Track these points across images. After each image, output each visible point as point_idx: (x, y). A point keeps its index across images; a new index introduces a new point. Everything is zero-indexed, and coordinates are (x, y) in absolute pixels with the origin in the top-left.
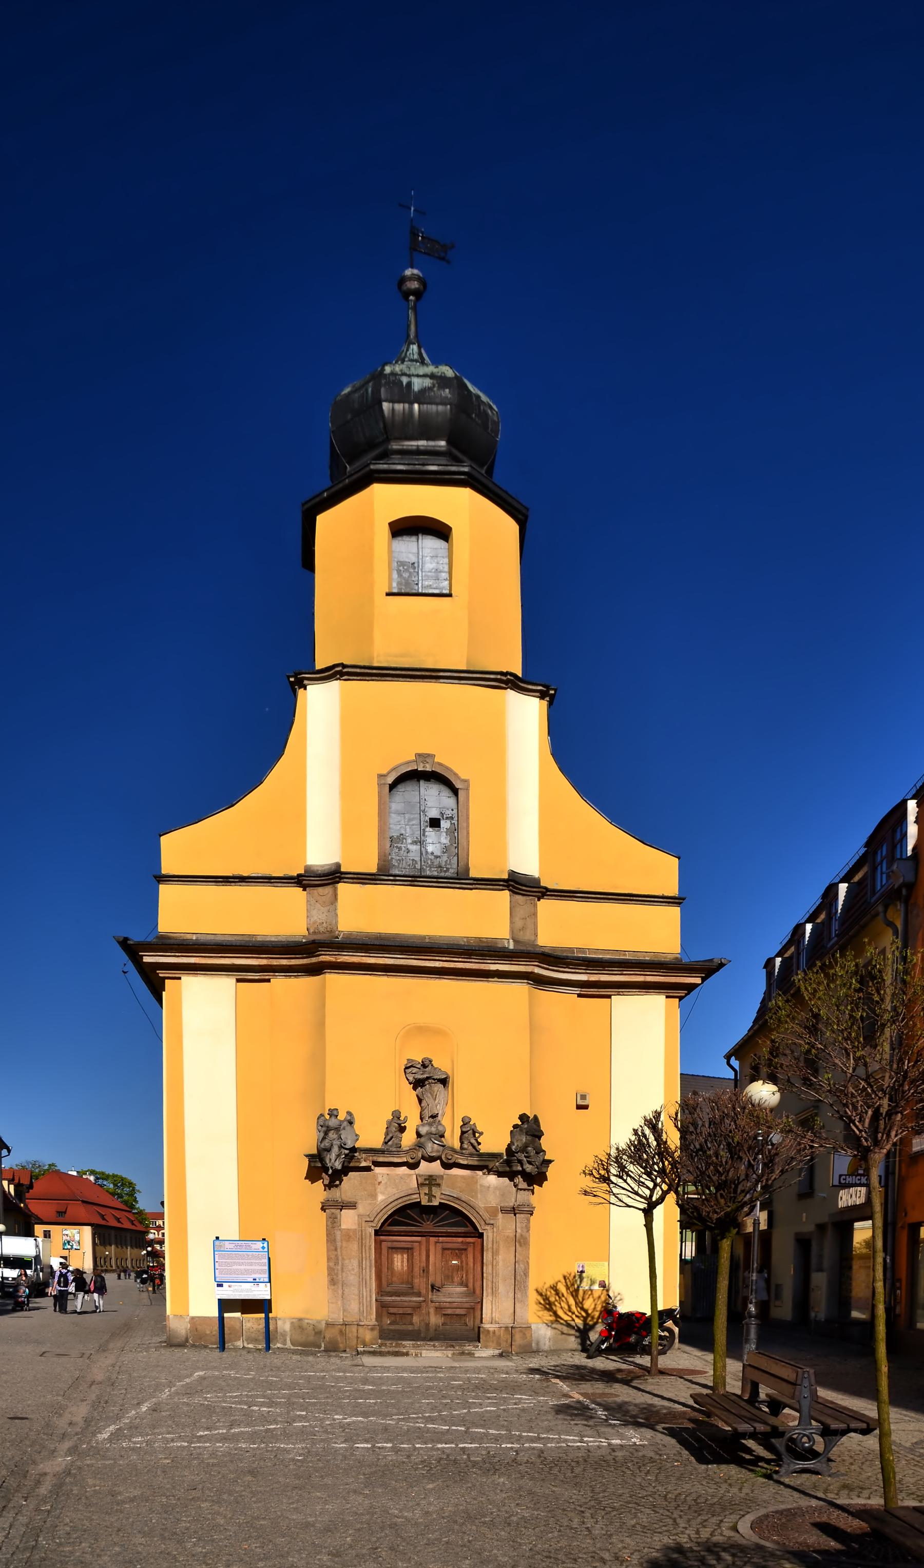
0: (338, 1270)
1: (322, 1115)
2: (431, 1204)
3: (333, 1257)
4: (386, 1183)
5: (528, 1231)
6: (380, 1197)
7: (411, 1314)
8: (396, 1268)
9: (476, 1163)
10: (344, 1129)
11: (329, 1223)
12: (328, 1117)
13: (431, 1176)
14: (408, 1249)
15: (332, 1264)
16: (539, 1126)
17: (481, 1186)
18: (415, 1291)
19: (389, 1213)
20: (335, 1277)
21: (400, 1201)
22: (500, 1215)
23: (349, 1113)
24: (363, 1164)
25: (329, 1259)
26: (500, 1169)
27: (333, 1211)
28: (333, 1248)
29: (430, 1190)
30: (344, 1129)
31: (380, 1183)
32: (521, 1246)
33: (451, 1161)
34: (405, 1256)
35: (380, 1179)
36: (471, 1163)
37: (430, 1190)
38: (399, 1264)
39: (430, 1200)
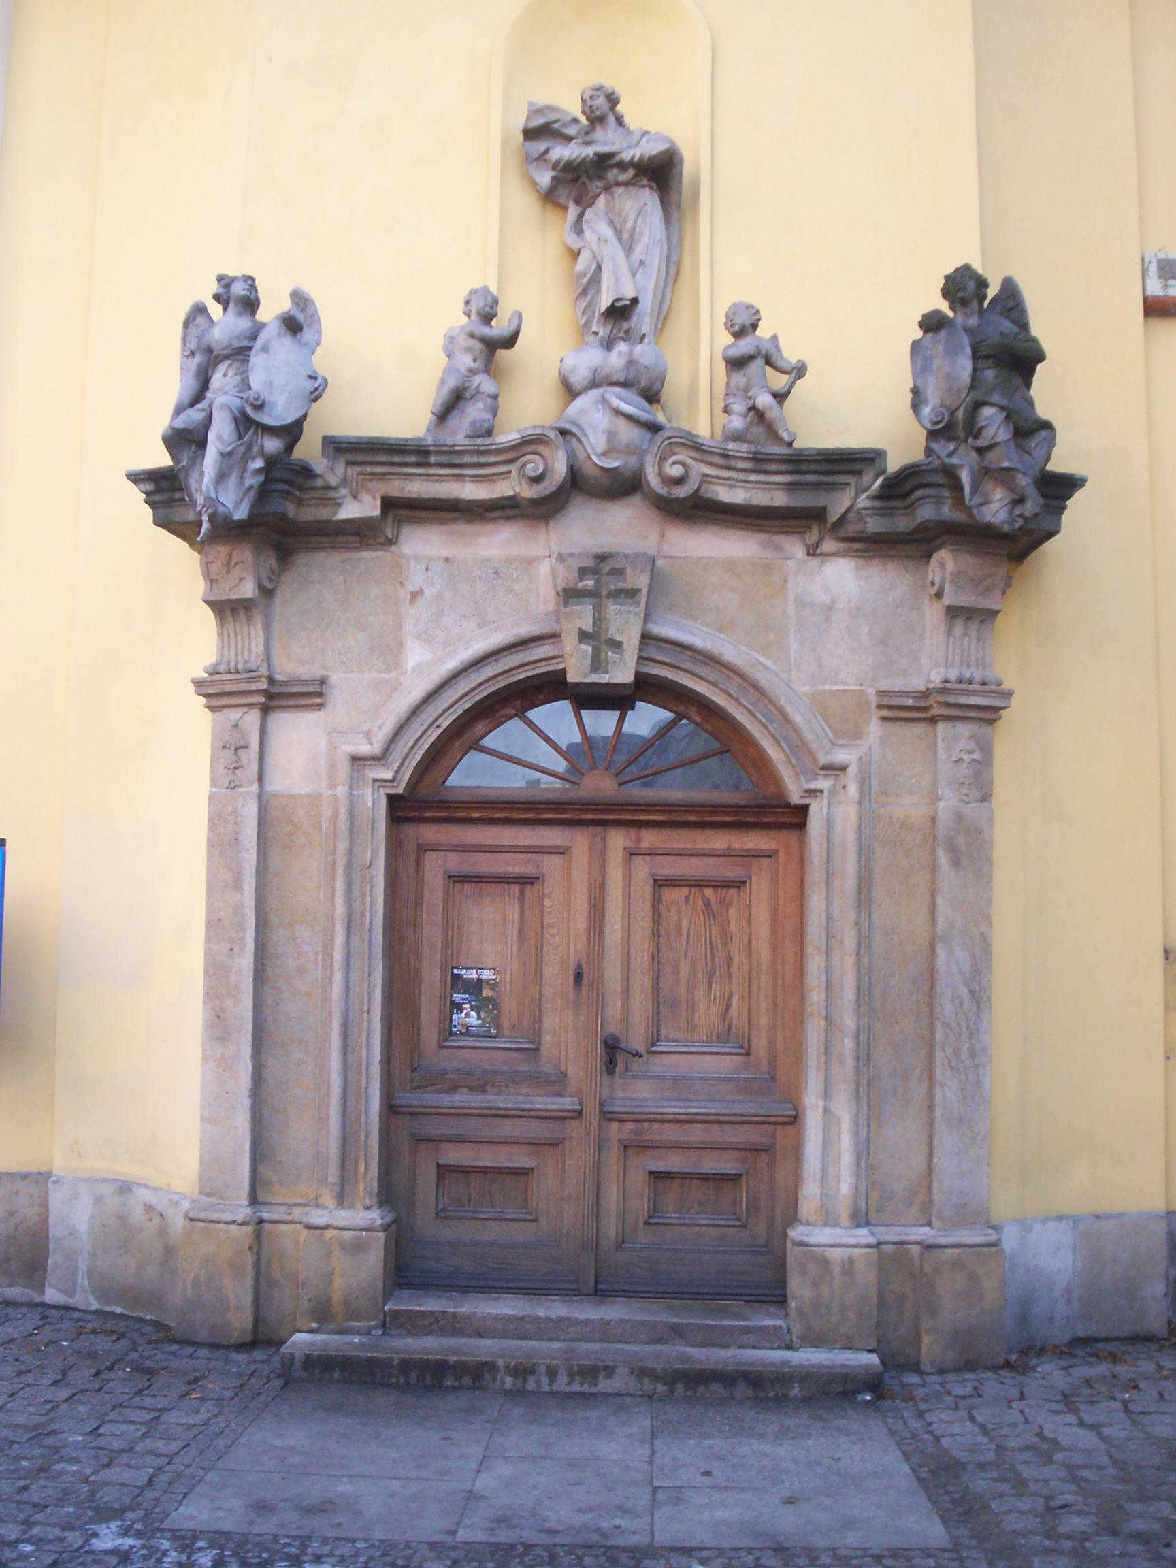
1: (199, 310)
2: (604, 678)
4: (439, 596)
5: (985, 798)
9: (779, 499)
11: (221, 771)
12: (215, 310)
13: (602, 558)
16: (1024, 326)
17: (800, 603)
19: (446, 723)
20: (229, 1002)
21: (489, 671)
22: (874, 729)
23: (299, 298)
24: (350, 511)
25: (213, 925)
26: (874, 525)
27: (235, 715)
29: (599, 618)
30: (265, 349)
31: (415, 596)
32: (956, 864)
33: (681, 492)
35: (416, 579)
36: (762, 498)
37: (599, 618)
39: (597, 664)
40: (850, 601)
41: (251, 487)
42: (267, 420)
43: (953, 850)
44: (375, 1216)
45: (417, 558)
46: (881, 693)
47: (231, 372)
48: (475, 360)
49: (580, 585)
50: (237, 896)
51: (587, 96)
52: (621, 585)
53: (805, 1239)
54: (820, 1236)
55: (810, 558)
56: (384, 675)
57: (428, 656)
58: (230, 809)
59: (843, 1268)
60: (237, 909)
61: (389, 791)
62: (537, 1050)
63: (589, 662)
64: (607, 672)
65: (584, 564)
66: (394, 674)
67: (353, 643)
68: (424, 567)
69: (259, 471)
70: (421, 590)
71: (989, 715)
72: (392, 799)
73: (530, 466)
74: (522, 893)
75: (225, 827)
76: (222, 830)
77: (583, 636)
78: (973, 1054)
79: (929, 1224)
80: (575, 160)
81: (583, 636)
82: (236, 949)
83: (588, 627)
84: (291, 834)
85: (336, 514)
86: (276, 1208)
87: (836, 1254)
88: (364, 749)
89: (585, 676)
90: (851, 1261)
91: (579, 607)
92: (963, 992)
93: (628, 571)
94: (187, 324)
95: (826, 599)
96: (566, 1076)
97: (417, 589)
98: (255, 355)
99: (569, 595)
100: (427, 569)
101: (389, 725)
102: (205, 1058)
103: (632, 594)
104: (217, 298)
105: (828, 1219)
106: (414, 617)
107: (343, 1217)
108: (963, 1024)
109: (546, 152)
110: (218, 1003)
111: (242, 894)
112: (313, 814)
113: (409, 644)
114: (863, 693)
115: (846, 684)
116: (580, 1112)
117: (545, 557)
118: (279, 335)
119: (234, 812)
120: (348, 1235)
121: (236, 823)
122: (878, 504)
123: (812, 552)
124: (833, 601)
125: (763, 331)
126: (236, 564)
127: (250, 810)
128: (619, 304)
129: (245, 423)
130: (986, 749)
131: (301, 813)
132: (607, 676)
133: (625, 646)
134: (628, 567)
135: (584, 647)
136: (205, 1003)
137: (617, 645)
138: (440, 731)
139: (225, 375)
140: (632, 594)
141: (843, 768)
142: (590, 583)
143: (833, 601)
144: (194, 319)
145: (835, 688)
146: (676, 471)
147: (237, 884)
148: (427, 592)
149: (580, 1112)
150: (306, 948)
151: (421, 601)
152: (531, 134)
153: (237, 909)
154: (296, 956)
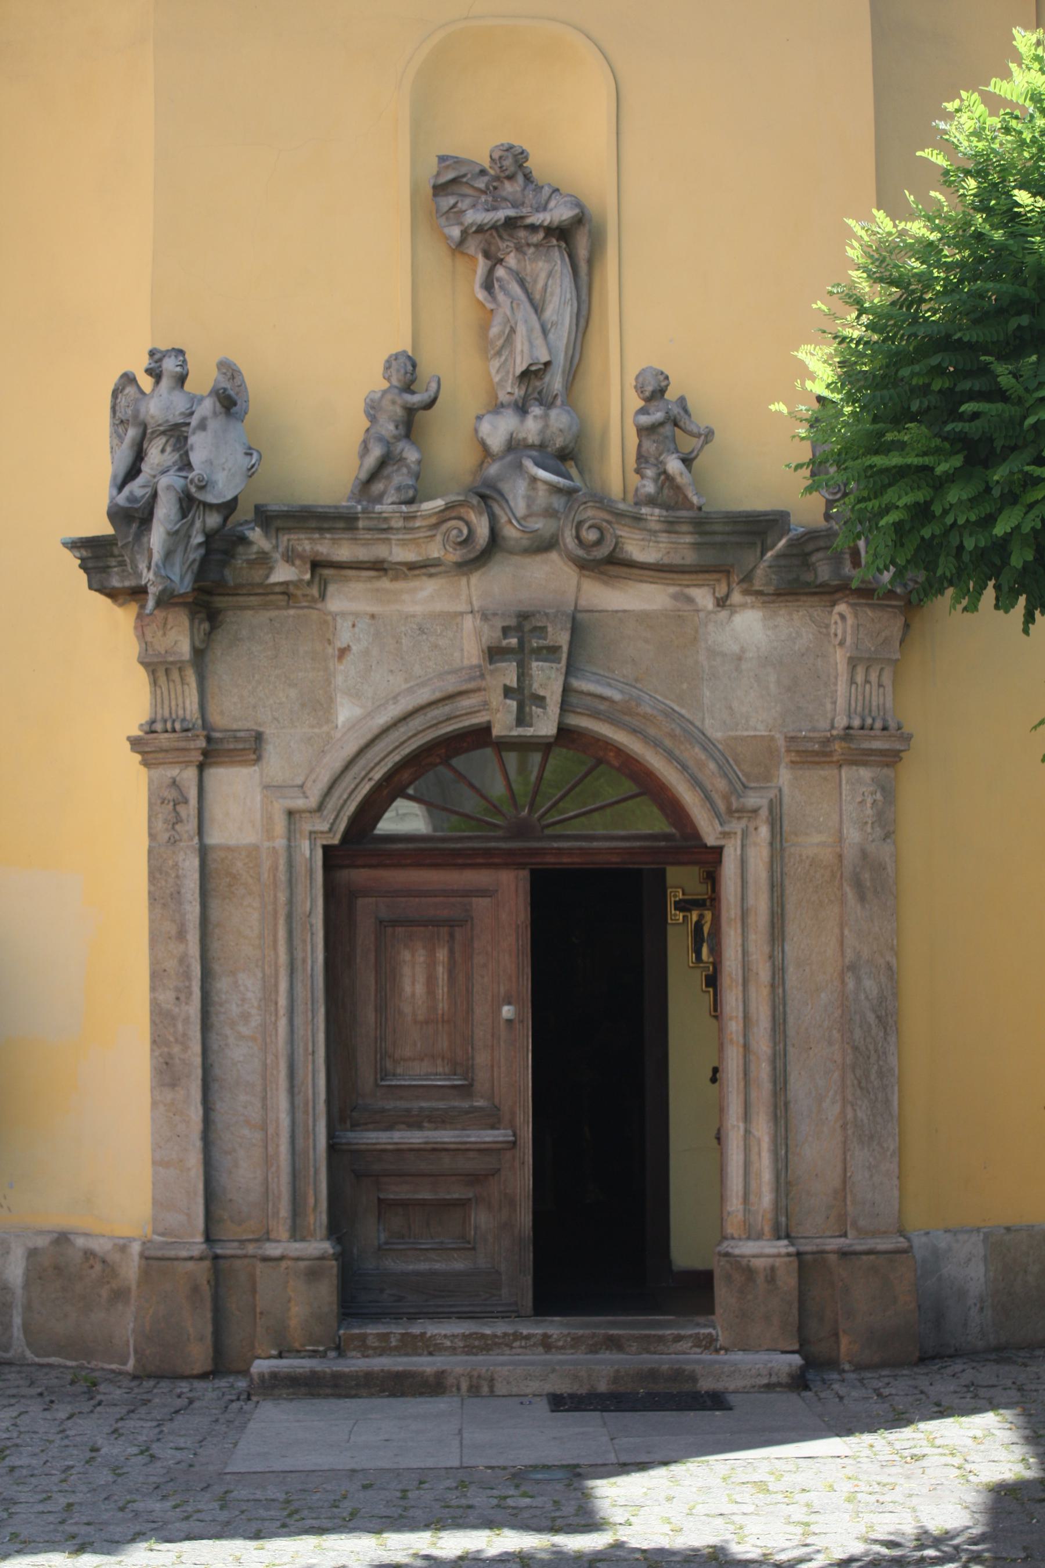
0: (187, 1020)
1: (128, 379)
2: (529, 731)
3: (171, 964)
4: (366, 652)
6: (345, 712)
7: (462, 1204)
8: (407, 1009)
10: (202, 426)
11: (160, 825)
12: (146, 383)
13: (524, 616)
14: (451, 924)
15: (167, 997)
17: (712, 653)
18: (480, 1103)
19: (378, 775)
20: (176, 1049)
21: (416, 723)
23: (229, 369)
24: (282, 573)
25: (157, 976)
28: (173, 930)
29: (523, 674)
31: (343, 652)
32: (862, 898)
34: (442, 955)
35: (344, 636)
37: (523, 674)
38: (420, 989)
39: (521, 720)
40: (758, 648)
41: (194, 560)
42: (211, 498)
43: (858, 885)
44: (326, 1247)
45: (343, 614)
46: (791, 739)
47: (169, 449)
48: (397, 427)
49: (505, 643)
50: (182, 947)
51: (496, 156)
52: (542, 643)
53: (730, 1250)
54: (747, 1248)
55: (719, 609)
56: (316, 730)
57: (358, 711)
58: (171, 863)
59: (766, 1277)
60: (183, 960)
61: (325, 843)
62: (471, 1085)
63: (514, 716)
64: (531, 726)
65: (506, 624)
66: (325, 728)
67: (284, 699)
68: (350, 624)
69: (200, 545)
70: (349, 646)
71: (891, 758)
72: (328, 851)
73: (455, 532)
74: (452, 936)
75: (166, 881)
76: (163, 883)
77: (508, 692)
78: (881, 1074)
79: (845, 1235)
80: (486, 224)
81: (508, 692)
82: (183, 997)
83: (512, 681)
84: (230, 885)
85: (267, 576)
86: (228, 1245)
87: (759, 1263)
88: (300, 803)
89: (511, 729)
90: (773, 1269)
91: (504, 664)
92: (871, 1017)
93: (550, 629)
94: (115, 393)
95: (736, 648)
96: (499, 1110)
97: (344, 645)
98: (194, 433)
99: (494, 654)
100: (354, 626)
101: (325, 778)
102: (154, 1104)
103: (553, 651)
104: (149, 371)
105: (752, 1234)
106: (345, 673)
107: (296, 1248)
108: (871, 1047)
109: (455, 206)
110: (166, 1050)
111: (187, 945)
112: (251, 865)
113: (338, 699)
114: (772, 739)
115: (755, 729)
116: (514, 1143)
117: (467, 613)
118: (215, 414)
119: (176, 865)
120: (302, 1264)
121: (177, 877)
122: (783, 562)
123: (722, 603)
124: (743, 650)
125: (671, 395)
126: (172, 628)
127: (191, 864)
128: (533, 368)
129: (187, 503)
130: (888, 793)
131: (239, 864)
132: (532, 729)
133: (548, 700)
134: (549, 625)
135: (508, 701)
136: (152, 1050)
137: (540, 701)
138: (372, 783)
139: (163, 451)
140: (553, 651)
141: (755, 811)
142: (514, 641)
143: (743, 650)
144: (123, 389)
145: (746, 733)
146: (592, 536)
147: (181, 935)
148: (354, 648)
149: (514, 1143)
150: (249, 995)
151: (349, 658)
152: (440, 189)
153: (183, 960)
154: (239, 1002)
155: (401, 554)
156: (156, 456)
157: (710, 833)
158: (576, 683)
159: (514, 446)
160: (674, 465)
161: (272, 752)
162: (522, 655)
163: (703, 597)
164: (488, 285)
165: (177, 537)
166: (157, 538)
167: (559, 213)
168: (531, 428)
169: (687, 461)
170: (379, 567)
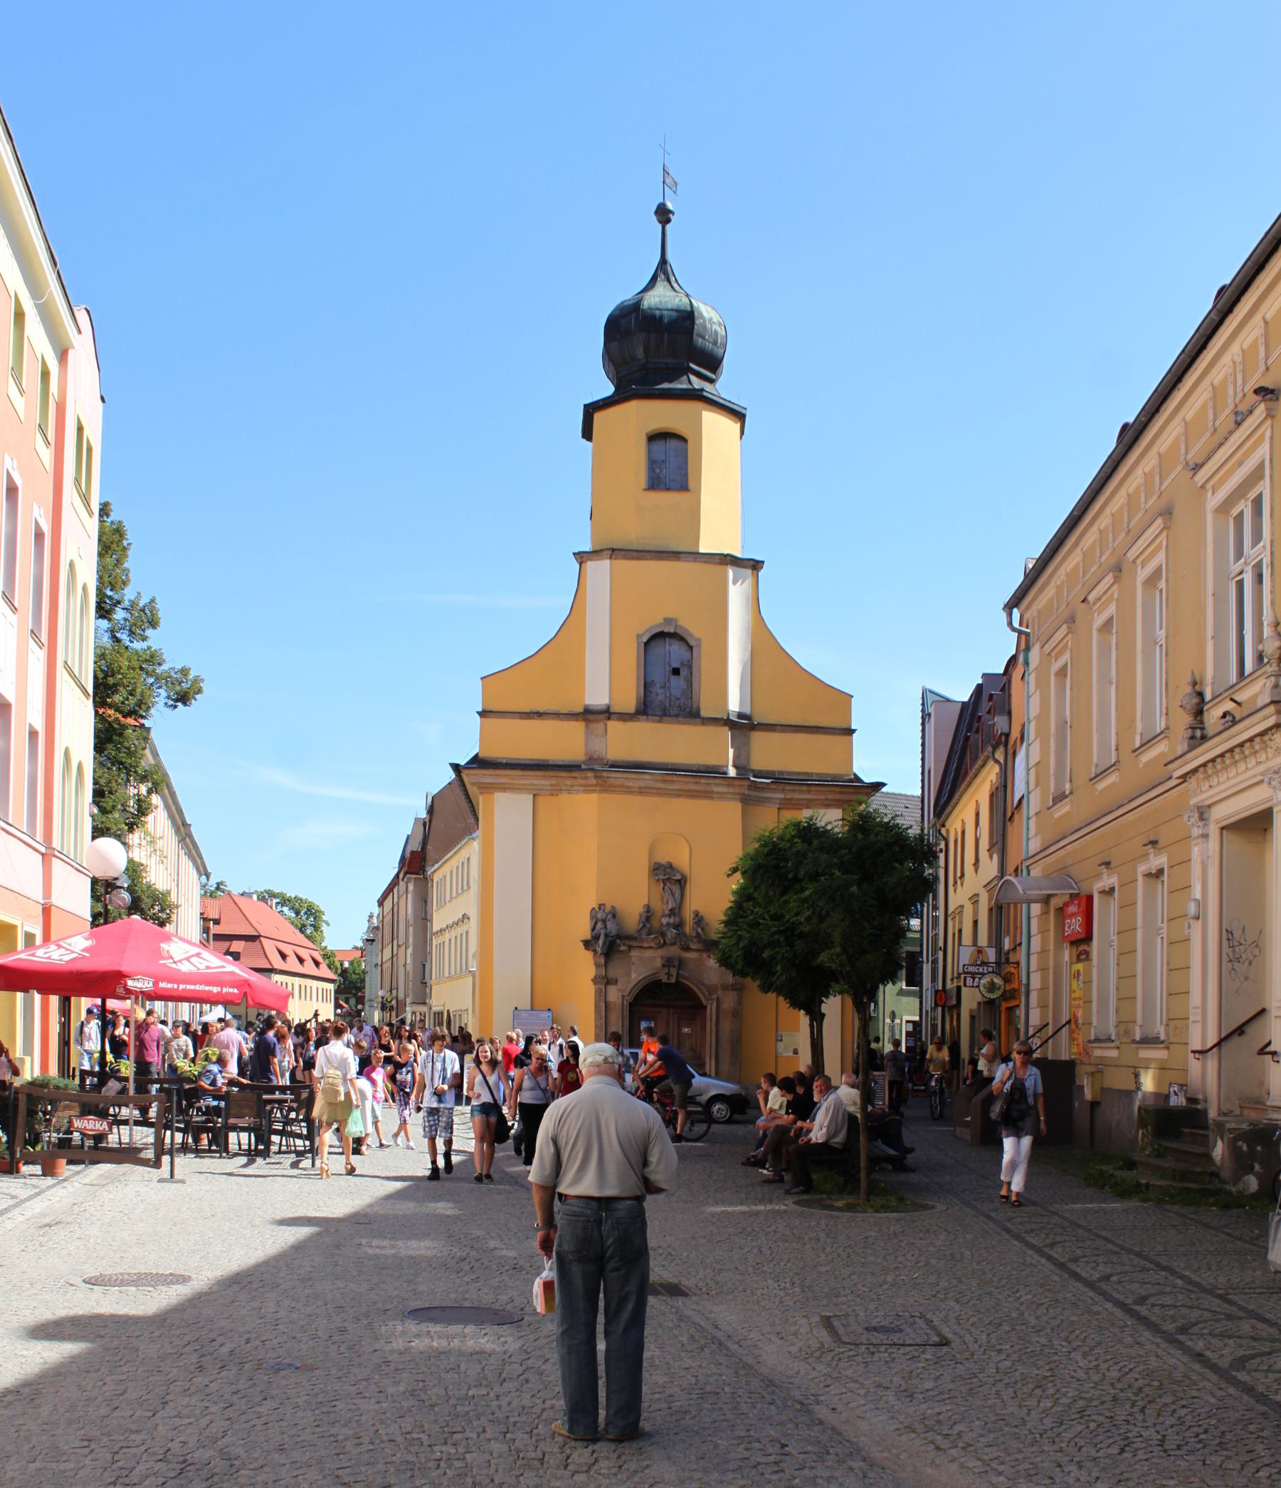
6: (634, 976)
24: (622, 948)
35: (634, 960)
99: (664, 966)
127: (603, 1005)
129: (606, 936)
155: (645, 945)
156: (600, 925)
157: (704, 1002)
158: (681, 972)
159: (668, 924)
160: (700, 930)
161: (619, 983)
162: (669, 967)
163: (705, 955)
164: (664, 889)
165: (604, 943)
166: (601, 942)
167: (678, 877)
168: (672, 921)
169: (702, 929)
170: (641, 947)
